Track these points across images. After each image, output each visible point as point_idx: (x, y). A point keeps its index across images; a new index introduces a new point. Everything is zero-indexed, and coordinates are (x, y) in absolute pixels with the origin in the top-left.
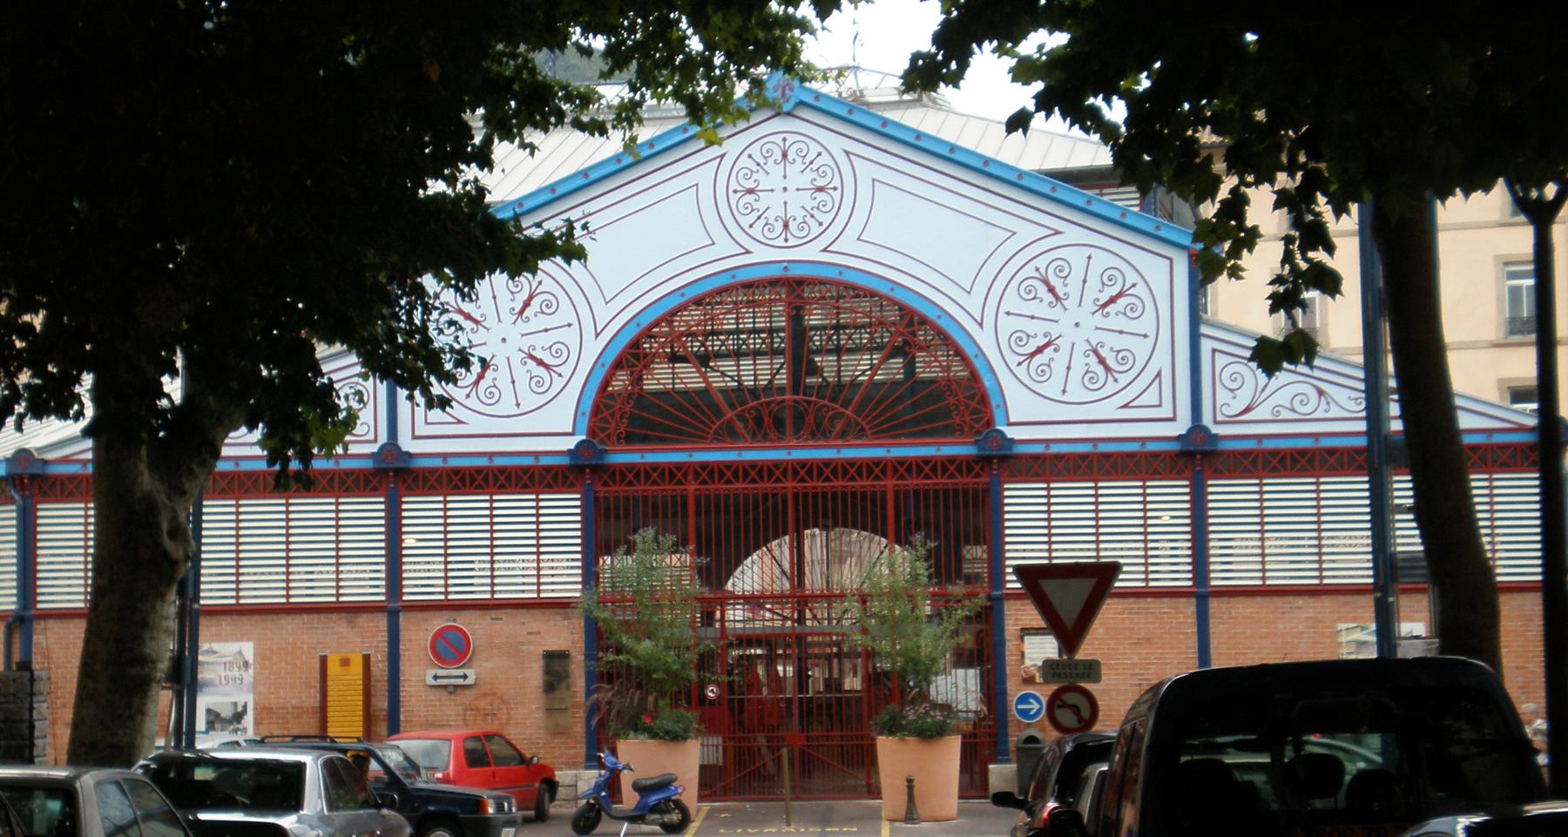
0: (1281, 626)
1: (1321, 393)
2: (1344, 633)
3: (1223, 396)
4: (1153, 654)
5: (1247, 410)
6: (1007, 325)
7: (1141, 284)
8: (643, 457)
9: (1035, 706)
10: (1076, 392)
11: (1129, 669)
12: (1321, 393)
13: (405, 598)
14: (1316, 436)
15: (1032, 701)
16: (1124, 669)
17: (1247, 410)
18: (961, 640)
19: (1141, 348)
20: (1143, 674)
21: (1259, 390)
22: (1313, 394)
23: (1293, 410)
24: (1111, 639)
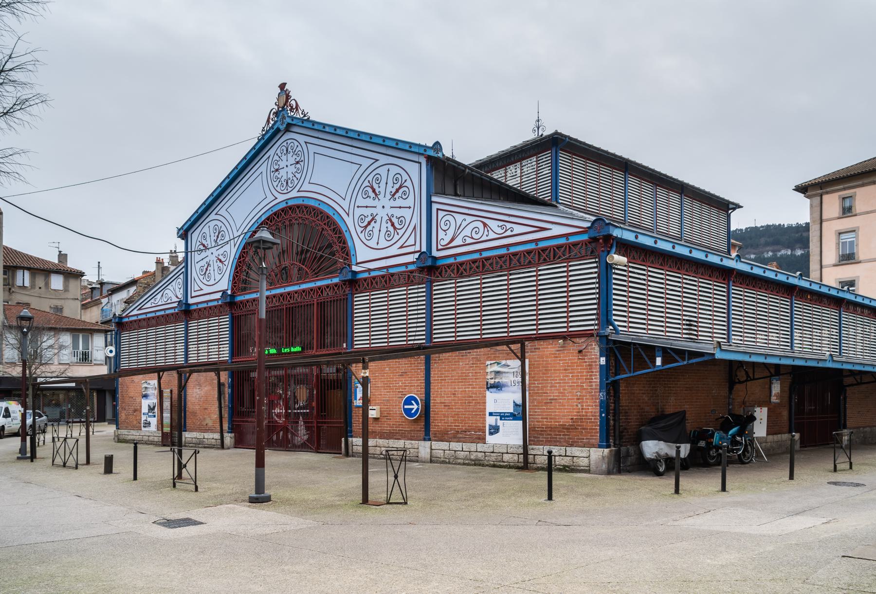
0: (461, 364)
1: (485, 225)
2: (489, 366)
3: (441, 234)
4: (407, 380)
5: (452, 240)
6: (358, 212)
7: (409, 180)
8: (331, 281)
9: (415, 407)
10: (383, 243)
11: (397, 389)
12: (485, 225)
13: (356, 347)
14: (507, 246)
15: (413, 402)
16: (396, 389)
17: (452, 240)
18: (496, 368)
19: (407, 213)
20: (403, 392)
21: (457, 228)
22: (481, 226)
23: (472, 238)
24: (391, 373)
